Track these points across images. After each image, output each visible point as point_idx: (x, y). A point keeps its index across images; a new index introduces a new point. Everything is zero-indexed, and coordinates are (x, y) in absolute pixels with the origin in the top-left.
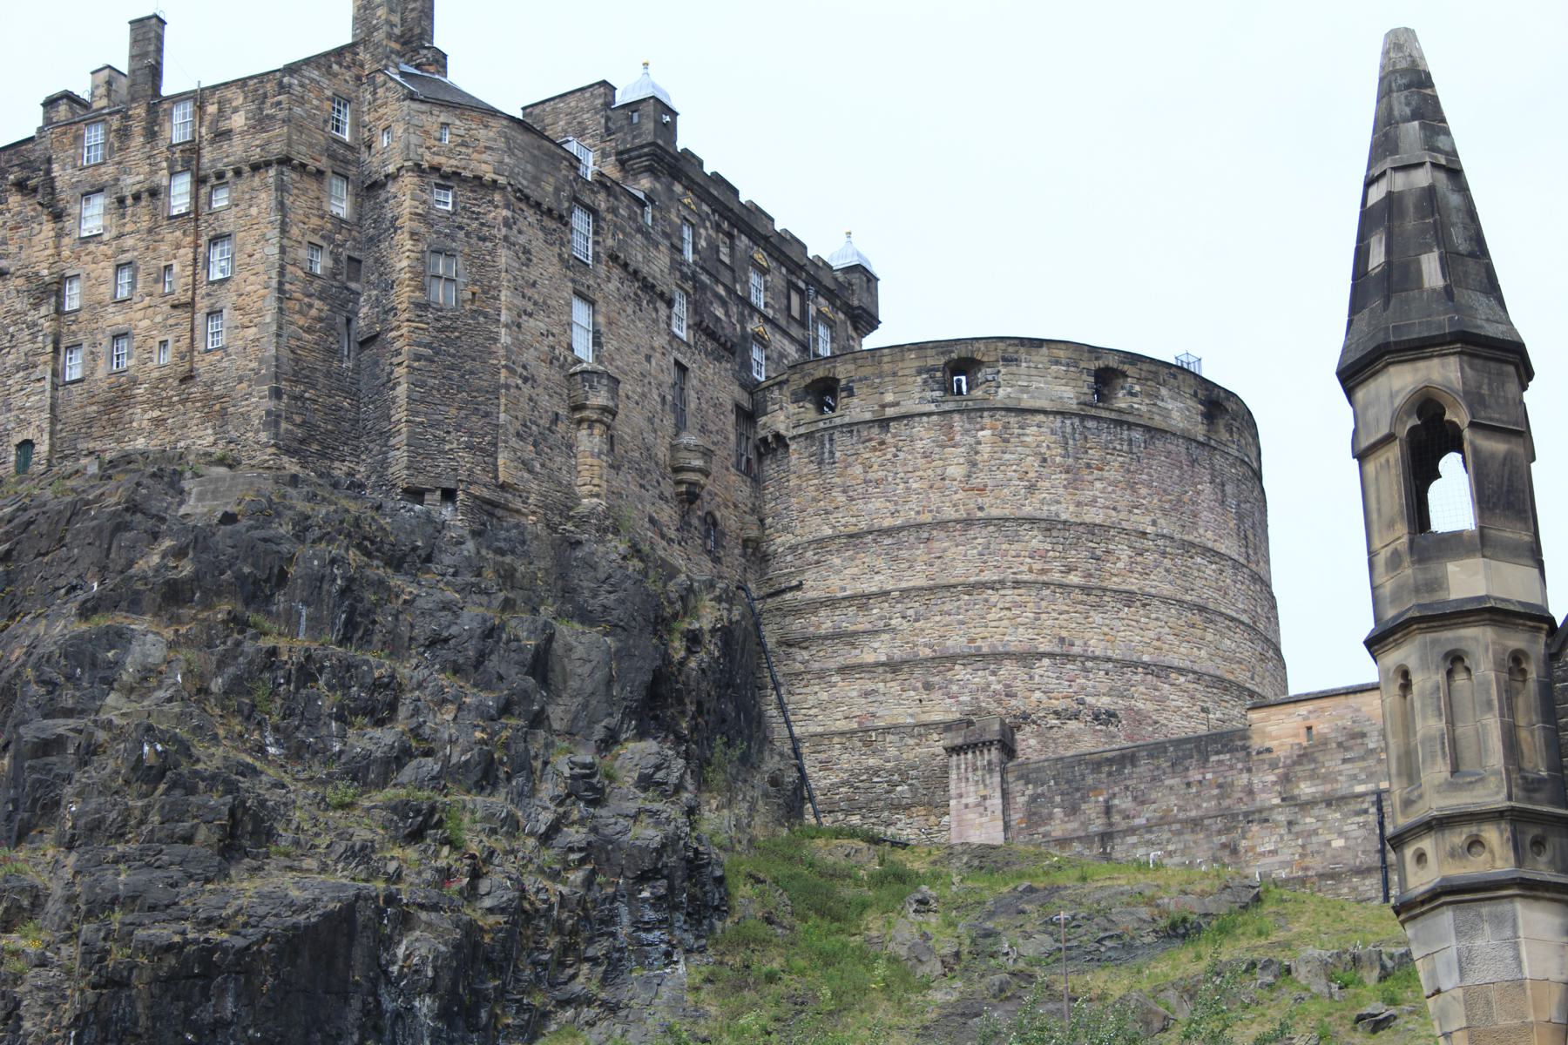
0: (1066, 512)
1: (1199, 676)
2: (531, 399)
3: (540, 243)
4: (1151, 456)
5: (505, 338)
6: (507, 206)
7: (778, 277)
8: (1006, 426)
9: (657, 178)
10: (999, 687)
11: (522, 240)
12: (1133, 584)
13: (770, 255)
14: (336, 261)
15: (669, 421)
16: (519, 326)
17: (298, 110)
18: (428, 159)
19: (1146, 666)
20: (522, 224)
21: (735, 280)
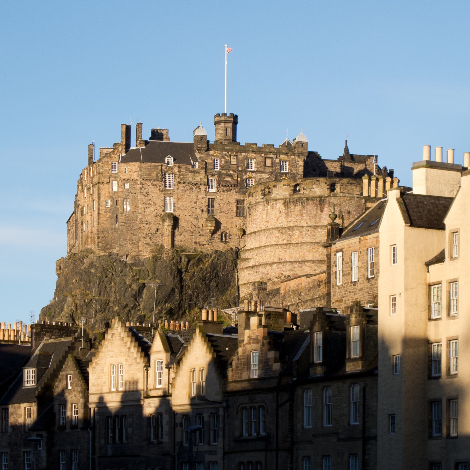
0: (285, 224)
1: (314, 262)
2: (149, 228)
3: (152, 189)
4: (308, 205)
6: (140, 184)
7: (260, 158)
8: (273, 204)
9: (202, 154)
10: (266, 272)
11: (146, 191)
12: (299, 240)
13: (255, 154)
14: (113, 202)
16: (145, 212)
17: (101, 170)
18: (123, 178)
19: (299, 262)
20: (145, 186)
21: (238, 167)
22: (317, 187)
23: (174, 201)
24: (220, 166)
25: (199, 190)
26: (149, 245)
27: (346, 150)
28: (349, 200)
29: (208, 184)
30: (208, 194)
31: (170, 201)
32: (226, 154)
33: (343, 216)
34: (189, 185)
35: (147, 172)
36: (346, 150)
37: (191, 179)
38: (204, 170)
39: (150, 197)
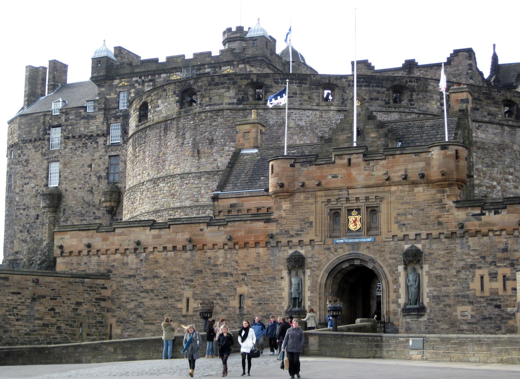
2: (27, 215)
5: (17, 199)
11: (25, 158)
15: (104, 185)
16: (23, 191)
22: (162, 103)
23: (60, 169)
24: (128, 101)
25: (95, 146)
26: (24, 241)
27: (495, 58)
28: (211, 117)
29: (108, 133)
30: (110, 149)
31: (55, 168)
32: (137, 81)
33: (198, 151)
34: (81, 140)
35: (27, 129)
36: (495, 58)
37: (82, 129)
38: (103, 112)
39: (30, 166)
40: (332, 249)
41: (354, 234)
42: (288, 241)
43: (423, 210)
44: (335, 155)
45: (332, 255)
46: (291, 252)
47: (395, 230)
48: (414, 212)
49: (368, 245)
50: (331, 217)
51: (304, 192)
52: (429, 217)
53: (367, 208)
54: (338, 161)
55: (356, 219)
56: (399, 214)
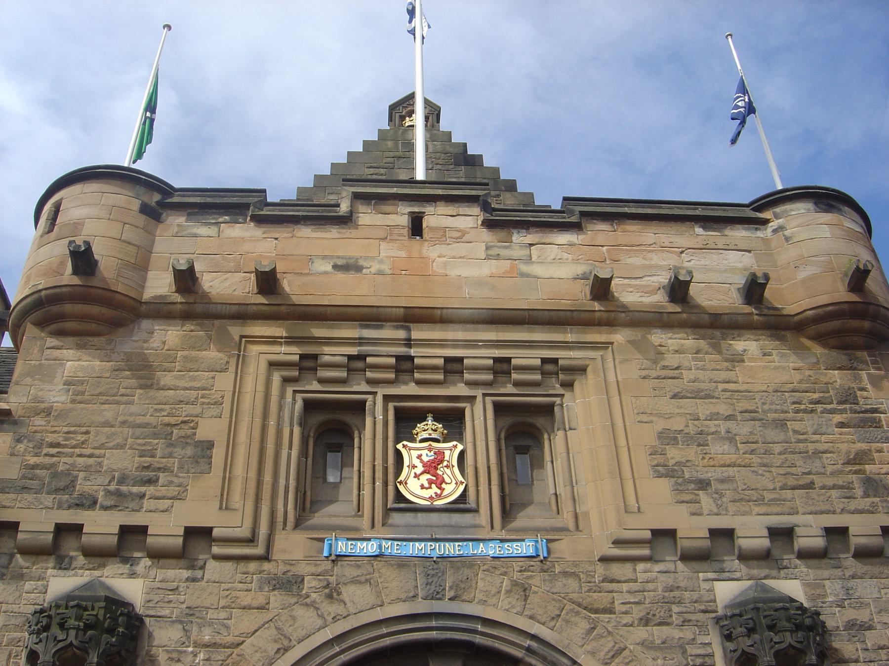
40: (310, 583)
41: (434, 518)
42: (62, 530)
43: (781, 424)
44: (357, 196)
45: (306, 618)
46: (60, 584)
47: (661, 507)
48: (743, 429)
49: (516, 576)
50: (304, 441)
51: (187, 316)
52: (817, 453)
53: (500, 409)
54: (367, 216)
55: (440, 454)
56: (668, 438)
